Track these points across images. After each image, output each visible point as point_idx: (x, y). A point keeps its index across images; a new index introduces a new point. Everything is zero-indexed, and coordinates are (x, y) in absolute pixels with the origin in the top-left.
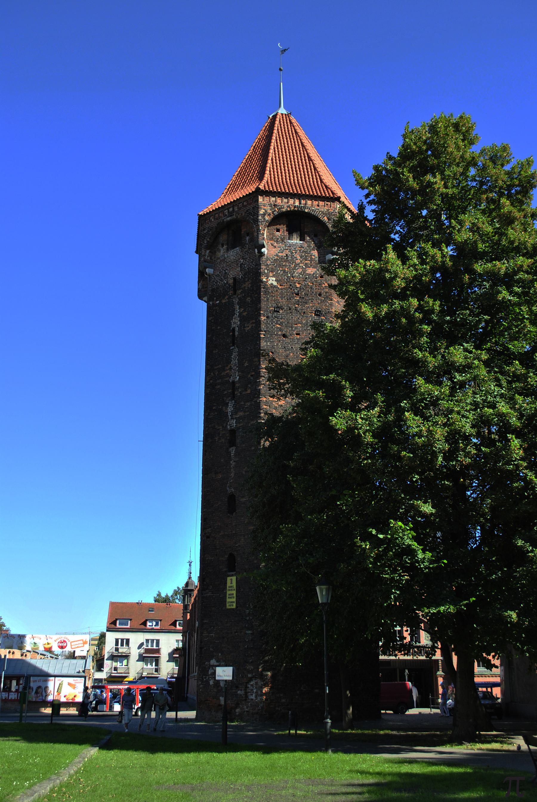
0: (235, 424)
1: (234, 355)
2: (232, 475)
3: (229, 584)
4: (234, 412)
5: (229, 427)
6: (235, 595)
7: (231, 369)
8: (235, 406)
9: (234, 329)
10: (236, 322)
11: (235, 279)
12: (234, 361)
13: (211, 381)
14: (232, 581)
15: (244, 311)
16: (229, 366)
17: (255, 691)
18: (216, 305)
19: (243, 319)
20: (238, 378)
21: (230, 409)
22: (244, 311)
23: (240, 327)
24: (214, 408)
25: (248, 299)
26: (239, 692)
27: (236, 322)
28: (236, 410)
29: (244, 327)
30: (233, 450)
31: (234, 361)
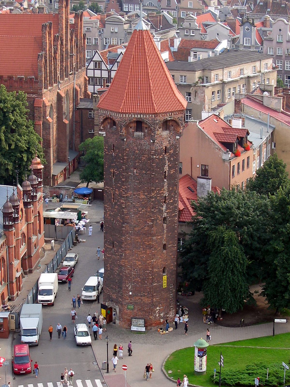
0: (166, 215)
1: (166, 184)
2: (165, 236)
3: (164, 279)
4: (166, 210)
5: (163, 216)
6: (166, 283)
7: (164, 190)
8: (166, 208)
9: (165, 172)
10: (166, 168)
11: (166, 147)
12: (166, 187)
13: (155, 195)
14: (165, 278)
15: (170, 164)
16: (163, 189)
17: (172, 313)
18: (157, 159)
19: (170, 168)
20: (167, 194)
21: (164, 208)
22: (170, 164)
23: (168, 171)
24: (157, 207)
25: (172, 159)
26: (168, 316)
27: (166, 168)
28: (167, 208)
29: (170, 172)
30: (165, 225)
31: (166, 187)
